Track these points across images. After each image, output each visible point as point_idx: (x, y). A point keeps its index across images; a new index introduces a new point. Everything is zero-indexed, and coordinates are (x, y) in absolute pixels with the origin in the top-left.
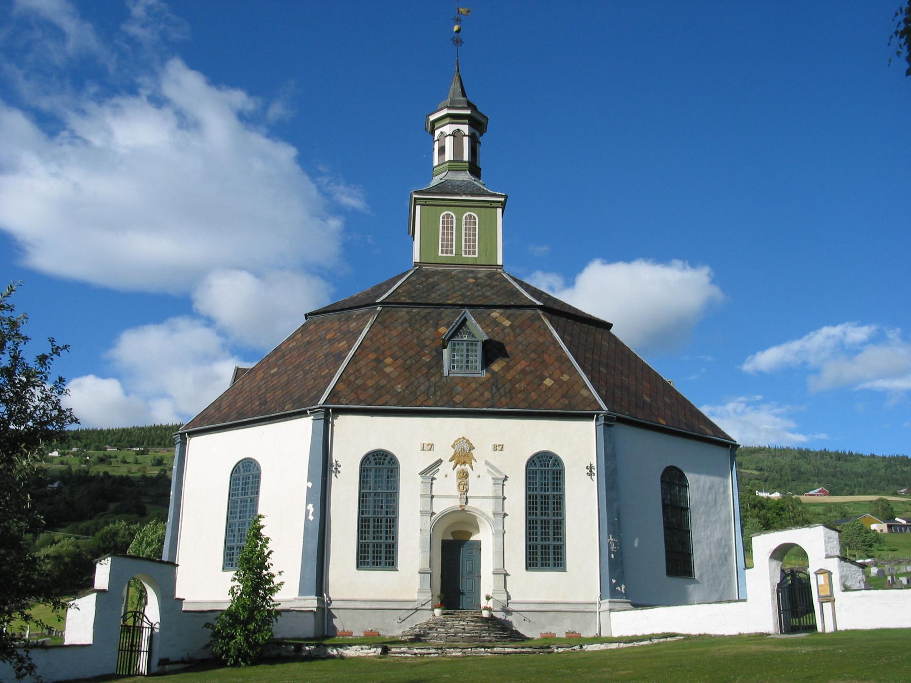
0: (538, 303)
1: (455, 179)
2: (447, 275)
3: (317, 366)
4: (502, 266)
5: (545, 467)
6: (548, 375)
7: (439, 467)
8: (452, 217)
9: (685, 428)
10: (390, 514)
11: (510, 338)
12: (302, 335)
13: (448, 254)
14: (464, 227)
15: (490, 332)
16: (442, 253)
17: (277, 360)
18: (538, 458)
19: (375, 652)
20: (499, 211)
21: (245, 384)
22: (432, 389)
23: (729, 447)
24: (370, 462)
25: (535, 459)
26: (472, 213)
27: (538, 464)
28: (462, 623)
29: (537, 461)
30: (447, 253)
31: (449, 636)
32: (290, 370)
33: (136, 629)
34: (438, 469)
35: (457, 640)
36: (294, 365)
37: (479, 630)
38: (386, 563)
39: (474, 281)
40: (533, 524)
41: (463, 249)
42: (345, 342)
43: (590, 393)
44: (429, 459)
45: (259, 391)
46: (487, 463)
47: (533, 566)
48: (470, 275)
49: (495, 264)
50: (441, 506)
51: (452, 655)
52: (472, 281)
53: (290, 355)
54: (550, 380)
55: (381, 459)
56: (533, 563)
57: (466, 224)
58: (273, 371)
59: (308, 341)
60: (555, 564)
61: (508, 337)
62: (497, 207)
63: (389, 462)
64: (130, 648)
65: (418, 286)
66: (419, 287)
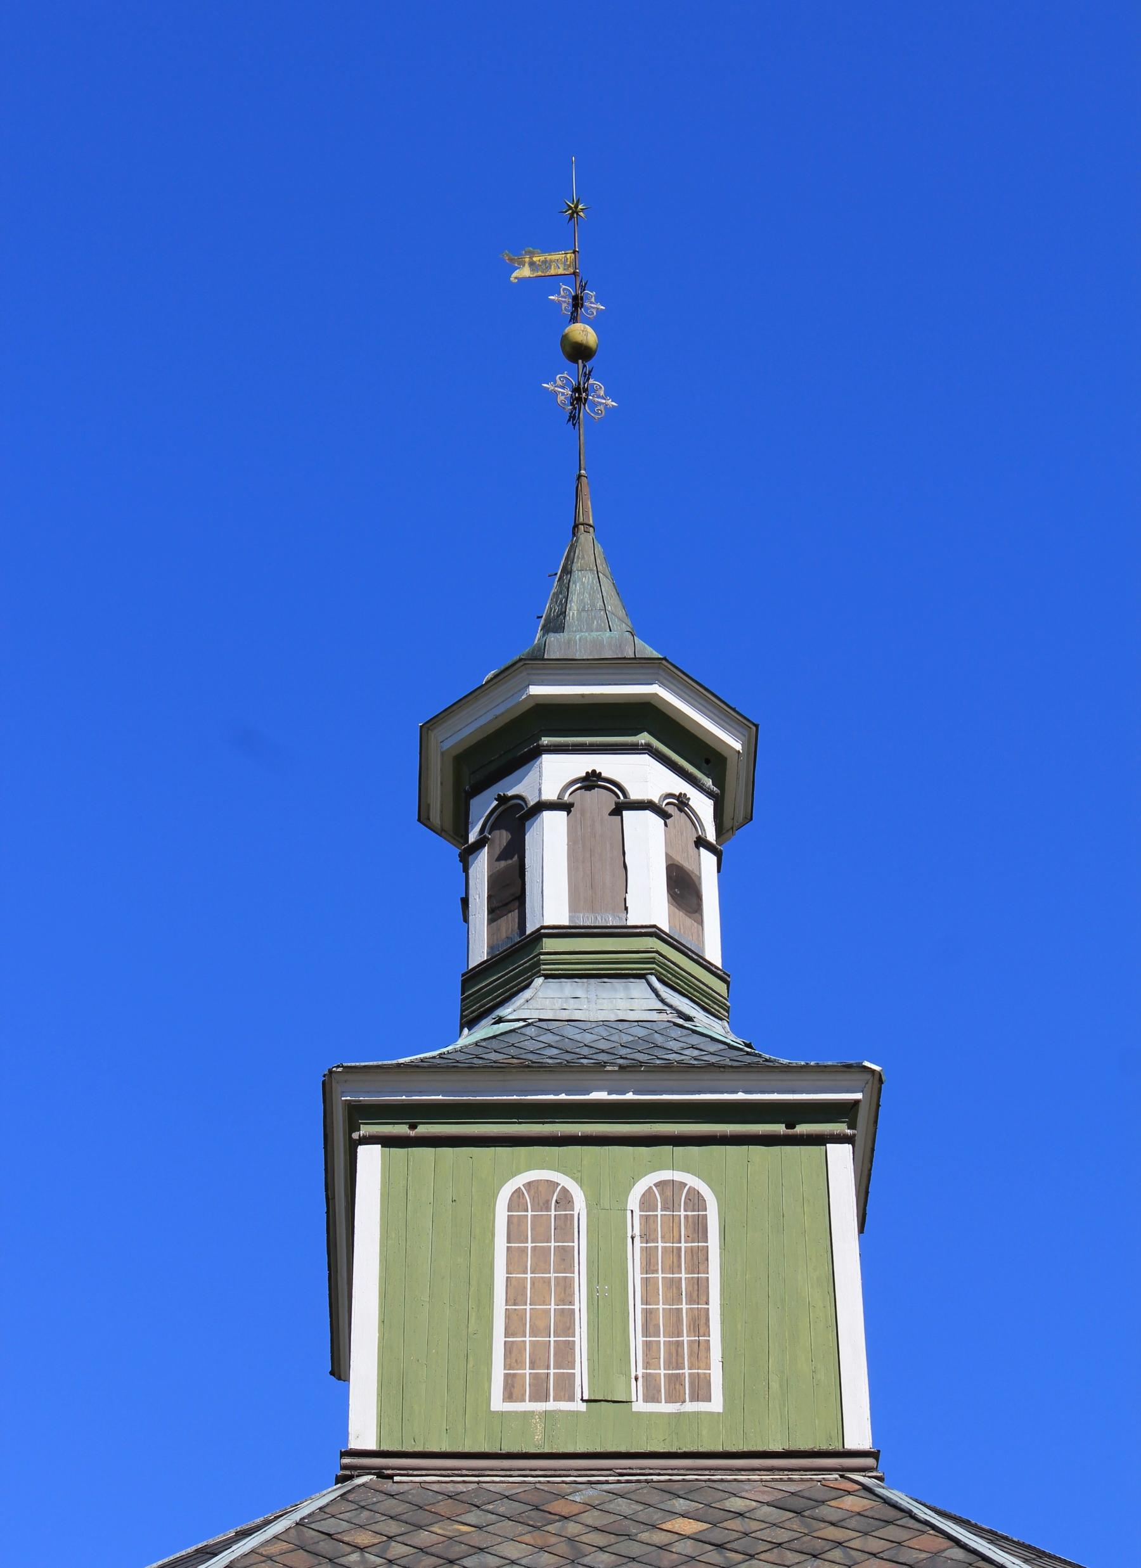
1: (577, 1015)
4: (874, 1455)
8: (566, 1199)
13: (547, 1399)
16: (510, 1394)
20: (841, 1157)
26: (679, 1176)
30: (540, 1394)
48: (680, 1505)
49: (836, 1446)
57: (647, 1236)
62: (820, 1140)
66: (364, 1561)
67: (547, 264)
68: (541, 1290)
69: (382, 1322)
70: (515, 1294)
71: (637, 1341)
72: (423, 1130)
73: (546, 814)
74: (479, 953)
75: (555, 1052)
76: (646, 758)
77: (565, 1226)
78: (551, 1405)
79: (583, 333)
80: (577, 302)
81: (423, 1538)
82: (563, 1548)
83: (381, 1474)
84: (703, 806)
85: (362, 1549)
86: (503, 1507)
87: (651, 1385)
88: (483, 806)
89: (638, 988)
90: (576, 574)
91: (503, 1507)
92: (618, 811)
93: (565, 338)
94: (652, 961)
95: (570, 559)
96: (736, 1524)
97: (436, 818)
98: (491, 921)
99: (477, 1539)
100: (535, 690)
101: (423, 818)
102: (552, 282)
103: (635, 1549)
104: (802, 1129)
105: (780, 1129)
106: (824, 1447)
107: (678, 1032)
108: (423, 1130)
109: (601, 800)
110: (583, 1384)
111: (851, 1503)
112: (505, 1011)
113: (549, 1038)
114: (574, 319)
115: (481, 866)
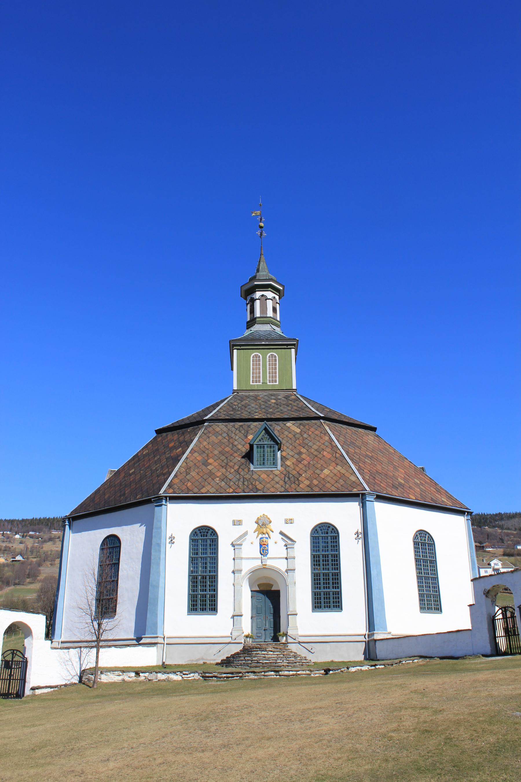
0: (322, 415)
1: (261, 330)
2: (256, 398)
3: (161, 466)
4: (296, 390)
5: (325, 534)
6: (326, 467)
8: (259, 357)
9: (432, 502)
11: (299, 441)
12: (152, 445)
14: (268, 363)
15: (285, 437)
16: (253, 383)
17: (134, 464)
18: (320, 527)
19: (193, 677)
20: (293, 351)
21: (112, 481)
22: (242, 480)
23: (465, 514)
24: (197, 535)
25: (318, 528)
28: (263, 652)
29: (319, 529)
30: (256, 382)
31: (253, 663)
32: (142, 471)
33: (14, 662)
34: (246, 539)
35: (258, 666)
36: (146, 466)
37: (276, 657)
38: (210, 608)
39: (275, 401)
40: (335, 576)
41: (268, 379)
42: (180, 449)
43: (357, 478)
44: (239, 531)
45: (120, 486)
46: (281, 533)
48: (273, 397)
49: (292, 389)
50: (247, 566)
51: (250, 678)
52: (274, 401)
53: (143, 460)
54: (327, 470)
55: (205, 533)
56: (318, 606)
58: (131, 472)
59: (157, 449)
60: (334, 606)
61: (298, 440)
62: (291, 348)
63: (211, 534)
64: (9, 677)
65: (235, 406)
66: (236, 407)
67: (257, 213)
68: (256, 368)
69: (237, 373)
70: (253, 369)
71: (268, 375)
72: (242, 347)
73: (257, 300)
74: (249, 319)
75: (258, 336)
76: (270, 292)
77: (259, 360)
78: (258, 384)
79: (262, 224)
80: (261, 219)
81: (243, 403)
82: (259, 405)
83: (237, 392)
84: (277, 297)
85: (235, 405)
86: (252, 398)
87: (269, 380)
88: (249, 298)
89: (268, 325)
90: (261, 262)
91: (252, 398)
92: (266, 300)
93: (259, 225)
94: (270, 321)
95: (260, 260)
96: (279, 401)
97: (243, 296)
98: (250, 314)
99: (249, 404)
100: (255, 283)
101: (241, 296)
102: (257, 216)
103: (267, 405)
104: (289, 347)
105: (286, 347)
106: (290, 389)
107: (273, 332)
108: (242, 347)
109: (263, 298)
110: (261, 381)
111: (293, 397)
112: (252, 329)
113: (257, 333)
114: (261, 222)
115: (249, 305)
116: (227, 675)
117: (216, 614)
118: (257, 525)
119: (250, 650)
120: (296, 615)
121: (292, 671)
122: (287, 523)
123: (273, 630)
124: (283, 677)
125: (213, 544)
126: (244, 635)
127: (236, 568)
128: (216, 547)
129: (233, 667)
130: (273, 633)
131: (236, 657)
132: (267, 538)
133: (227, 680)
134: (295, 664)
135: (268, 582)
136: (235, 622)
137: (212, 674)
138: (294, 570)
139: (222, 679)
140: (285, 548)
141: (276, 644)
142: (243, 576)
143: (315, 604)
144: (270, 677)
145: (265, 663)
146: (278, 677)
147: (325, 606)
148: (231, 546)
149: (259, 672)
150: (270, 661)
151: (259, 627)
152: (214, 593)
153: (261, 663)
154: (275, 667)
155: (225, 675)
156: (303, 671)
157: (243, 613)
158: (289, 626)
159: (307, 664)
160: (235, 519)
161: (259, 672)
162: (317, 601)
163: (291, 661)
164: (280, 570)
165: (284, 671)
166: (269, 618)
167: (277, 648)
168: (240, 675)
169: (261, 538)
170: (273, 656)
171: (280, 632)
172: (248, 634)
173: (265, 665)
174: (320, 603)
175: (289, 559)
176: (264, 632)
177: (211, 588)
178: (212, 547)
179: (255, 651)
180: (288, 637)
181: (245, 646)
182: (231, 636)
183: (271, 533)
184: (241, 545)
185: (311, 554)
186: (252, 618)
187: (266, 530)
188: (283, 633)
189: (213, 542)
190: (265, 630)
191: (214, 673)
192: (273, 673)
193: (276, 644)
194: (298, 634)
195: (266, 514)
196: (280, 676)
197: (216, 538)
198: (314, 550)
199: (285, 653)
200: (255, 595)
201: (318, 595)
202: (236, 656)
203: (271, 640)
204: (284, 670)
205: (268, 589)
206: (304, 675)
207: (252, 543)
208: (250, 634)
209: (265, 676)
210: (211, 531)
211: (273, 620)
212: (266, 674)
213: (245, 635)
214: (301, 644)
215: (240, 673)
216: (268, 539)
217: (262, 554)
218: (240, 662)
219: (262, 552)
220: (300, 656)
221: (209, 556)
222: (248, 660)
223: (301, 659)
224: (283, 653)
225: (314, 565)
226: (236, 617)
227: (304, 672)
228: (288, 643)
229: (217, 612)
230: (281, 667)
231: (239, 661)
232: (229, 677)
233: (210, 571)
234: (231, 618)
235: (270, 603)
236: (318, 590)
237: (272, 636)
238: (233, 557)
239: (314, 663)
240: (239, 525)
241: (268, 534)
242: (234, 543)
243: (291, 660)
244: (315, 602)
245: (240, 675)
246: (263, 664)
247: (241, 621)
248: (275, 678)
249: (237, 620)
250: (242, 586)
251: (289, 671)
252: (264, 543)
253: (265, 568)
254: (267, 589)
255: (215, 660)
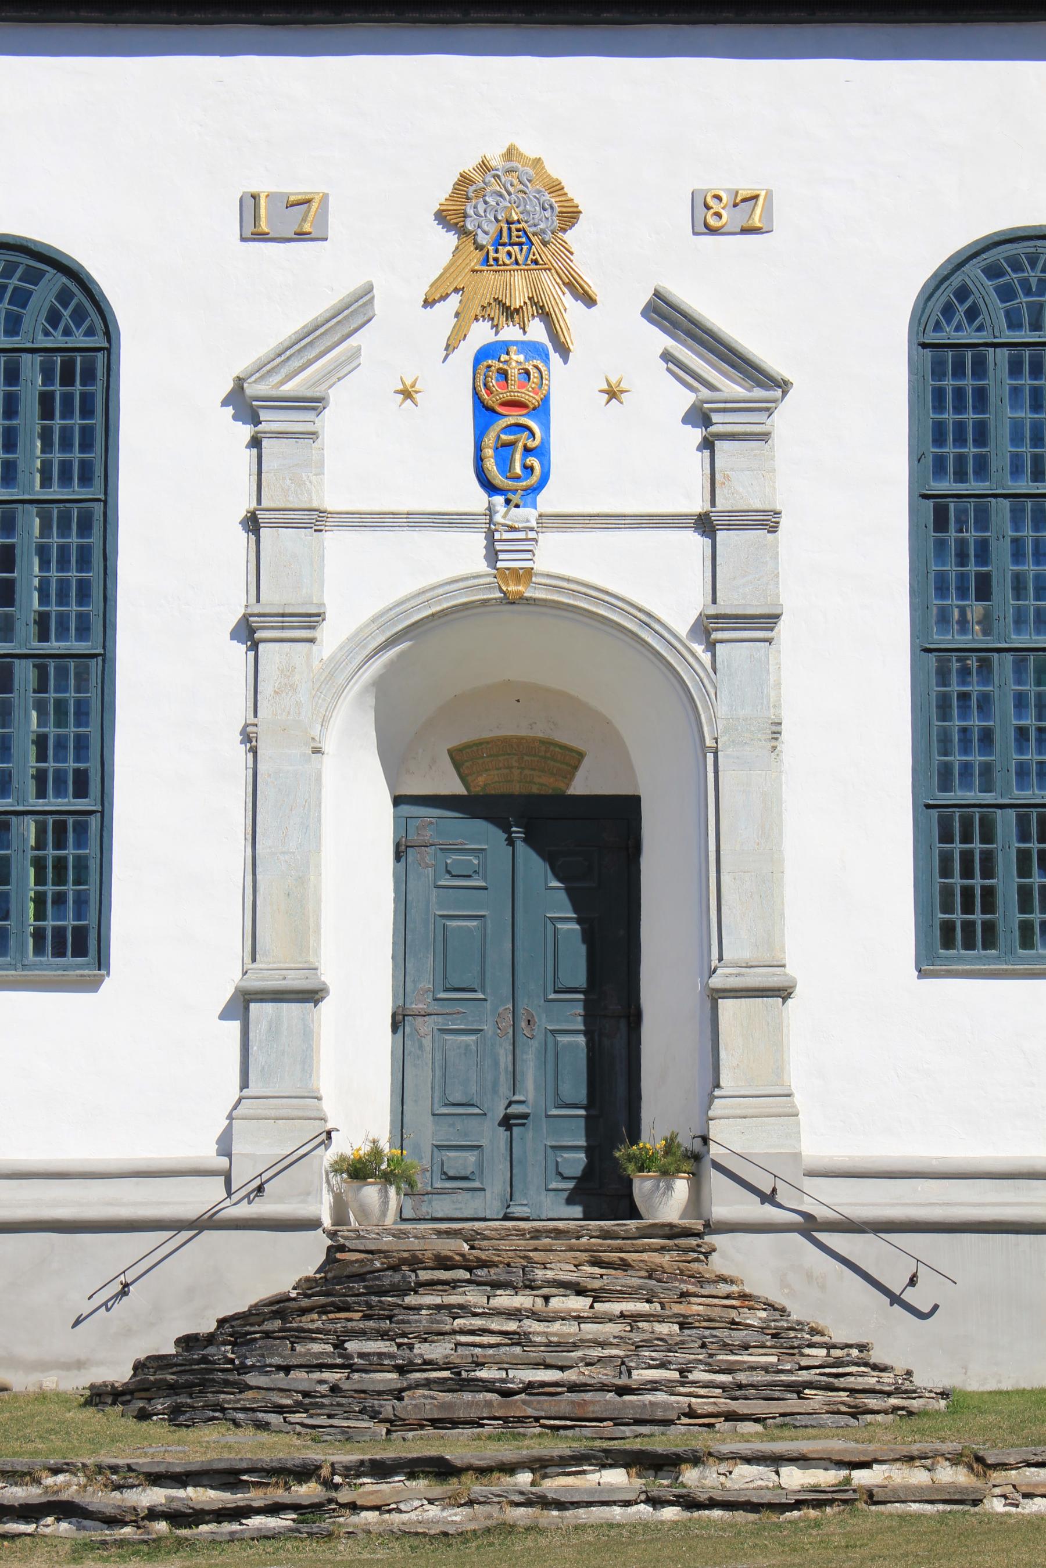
7: (353, 342)
10: (63, 633)
18: (993, 272)
25: (974, 271)
27: (995, 309)
28: (504, 1300)
29: (985, 289)
31: (417, 1386)
34: (357, 352)
35: (461, 1414)
37: (621, 1341)
38: (39, 935)
47: (969, 945)
63: (54, 318)
116: (180, 1493)
117: (93, 985)
118: (451, 239)
119: (390, 1278)
120: (784, 993)
121: (801, 1460)
122: (712, 231)
123: (582, 1123)
124: (717, 1513)
125: (67, 399)
126: (329, 1156)
127: (273, 599)
128: (97, 421)
129: (236, 1424)
130: (589, 1150)
131: (267, 1335)
132: (534, 350)
133: (180, 1543)
134: (792, 1404)
135: (540, 732)
136: (254, 1049)
137: (38, 1482)
138: (778, 617)
139: (127, 1530)
140: (697, 435)
141: (606, 1235)
142: (333, 666)
143: (947, 907)
144: (599, 1513)
145: (529, 1388)
146: (670, 1513)
147: (1026, 928)
148: (230, 410)
149: (483, 1471)
150: (571, 1376)
151: (457, 1097)
152: (81, 804)
153: (487, 1386)
154: (618, 1422)
155: (155, 1496)
156: (909, 1459)
157: (328, 975)
158: (718, 1086)
159: (893, 1401)
160: (263, 186)
161: (483, 1471)
162: (957, 881)
163: (759, 1377)
164: (648, 620)
165: (721, 1458)
166: (544, 1023)
167: (625, 1266)
168: (307, 1491)
169: (484, 354)
170: (590, 1329)
171: (634, 1136)
172: (366, 1149)
173: (522, 1405)
174: (989, 906)
175: (729, 527)
176: (502, 1134)
177: (51, 765)
178: (58, 422)
179: (431, 1284)
180: (714, 1173)
181: (342, 1248)
182: (223, 1162)
183: (571, 310)
184: (314, 404)
185: (920, 496)
186: (398, 1022)
187: (534, 285)
188: (670, 1147)
189: (68, 379)
190: (507, 1122)
191: (56, 1471)
192: (616, 1477)
193: (606, 1235)
194: (797, 1156)
195: (529, 149)
196: (689, 1503)
197: (99, 342)
198: (939, 466)
199: (696, 1308)
200: (428, 835)
201: (967, 838)
202: (268, 1326)
203: (570, 1201)
204: (725, 1448)
205: (542, 784)
206: (915, 1507)
207: (407, 394)
208: (385, 1146)
209: (546, 1503)
210: (54, 281)
211: (581, 1039)
212: (555, 1485)
213: (343, 1158)
214: (822, 1237)
215: (305, 1473)
216: (546, 358)
217: (489, 486)
218: (300, 1378)
219: (490, 465)
220: (816, 1339)
221: (38, 492)
222: (374, 1363)
223: (838, 1363)
224: (677, 1309)
225: (942, 589)
226: (269, 1007)
227: (918, 1477)
228: (711, 1228)
229: (102, 962)
230: (668, 1423)
231: (287, 1369)
232: (194, 1517)
233: (42, 621)
234: (225, 1015)
235: (563, 896)
236: (974, 796)
237: (577, 1171)
238: (245, 503)
239: (944, 1395)
240: (301, 236)
241: (546, 316)
242: (252, 389)
243: (752, 1368)
244: (947, 893)
245: (307, 1491)
246: (507, 1394)
247: (308, 1035)
248: (646, 1526)
249: (274, 1029)
250: (317, 751)
251: (776, 1461)
252: (515, 391)
253: (521, 600)
254: (535, 790)
255: (80, 1365)
